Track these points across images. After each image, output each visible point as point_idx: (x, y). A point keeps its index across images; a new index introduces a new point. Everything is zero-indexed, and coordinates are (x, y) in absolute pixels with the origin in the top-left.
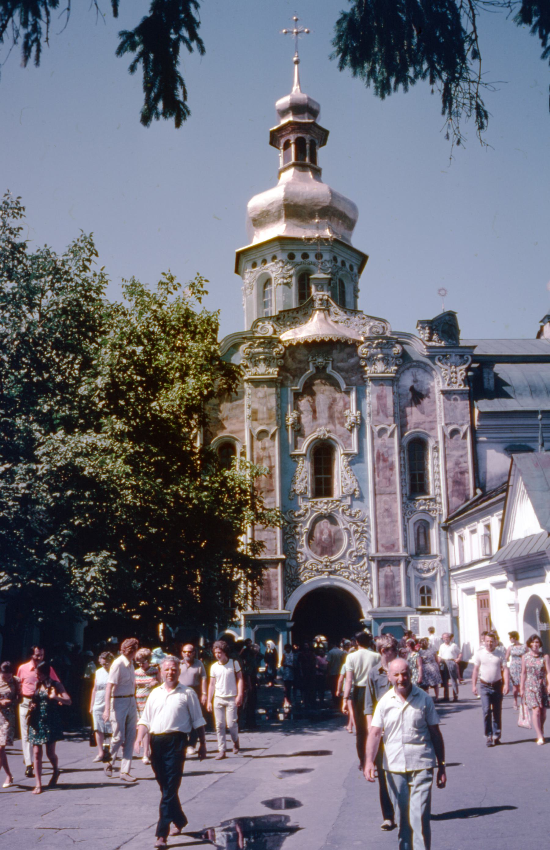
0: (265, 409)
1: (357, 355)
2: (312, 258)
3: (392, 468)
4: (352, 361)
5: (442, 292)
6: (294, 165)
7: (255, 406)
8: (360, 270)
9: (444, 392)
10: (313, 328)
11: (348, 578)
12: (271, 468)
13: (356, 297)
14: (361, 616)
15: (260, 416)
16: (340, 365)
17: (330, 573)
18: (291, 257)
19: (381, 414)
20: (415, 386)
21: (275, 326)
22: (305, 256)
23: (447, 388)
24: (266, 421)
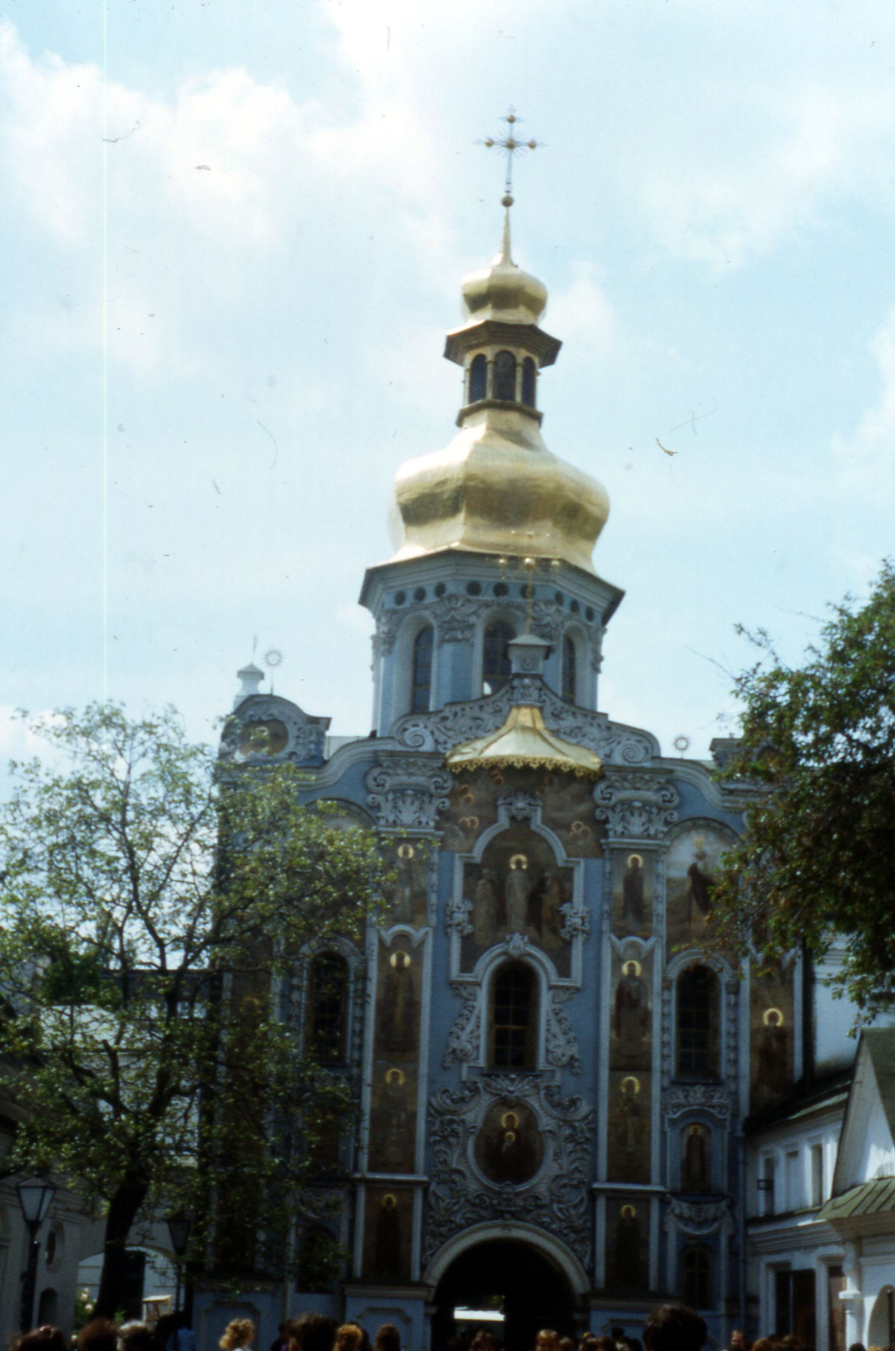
0: (407, 892)
1: (592, 800)
3: (645, 1020)
4: (583, 808)
11: (544, 1227)
13: (596, 670)
16: (556, 815)
18: (474, 588)
19: (630, 916)
20: (700, 866)
21: (436, 733)
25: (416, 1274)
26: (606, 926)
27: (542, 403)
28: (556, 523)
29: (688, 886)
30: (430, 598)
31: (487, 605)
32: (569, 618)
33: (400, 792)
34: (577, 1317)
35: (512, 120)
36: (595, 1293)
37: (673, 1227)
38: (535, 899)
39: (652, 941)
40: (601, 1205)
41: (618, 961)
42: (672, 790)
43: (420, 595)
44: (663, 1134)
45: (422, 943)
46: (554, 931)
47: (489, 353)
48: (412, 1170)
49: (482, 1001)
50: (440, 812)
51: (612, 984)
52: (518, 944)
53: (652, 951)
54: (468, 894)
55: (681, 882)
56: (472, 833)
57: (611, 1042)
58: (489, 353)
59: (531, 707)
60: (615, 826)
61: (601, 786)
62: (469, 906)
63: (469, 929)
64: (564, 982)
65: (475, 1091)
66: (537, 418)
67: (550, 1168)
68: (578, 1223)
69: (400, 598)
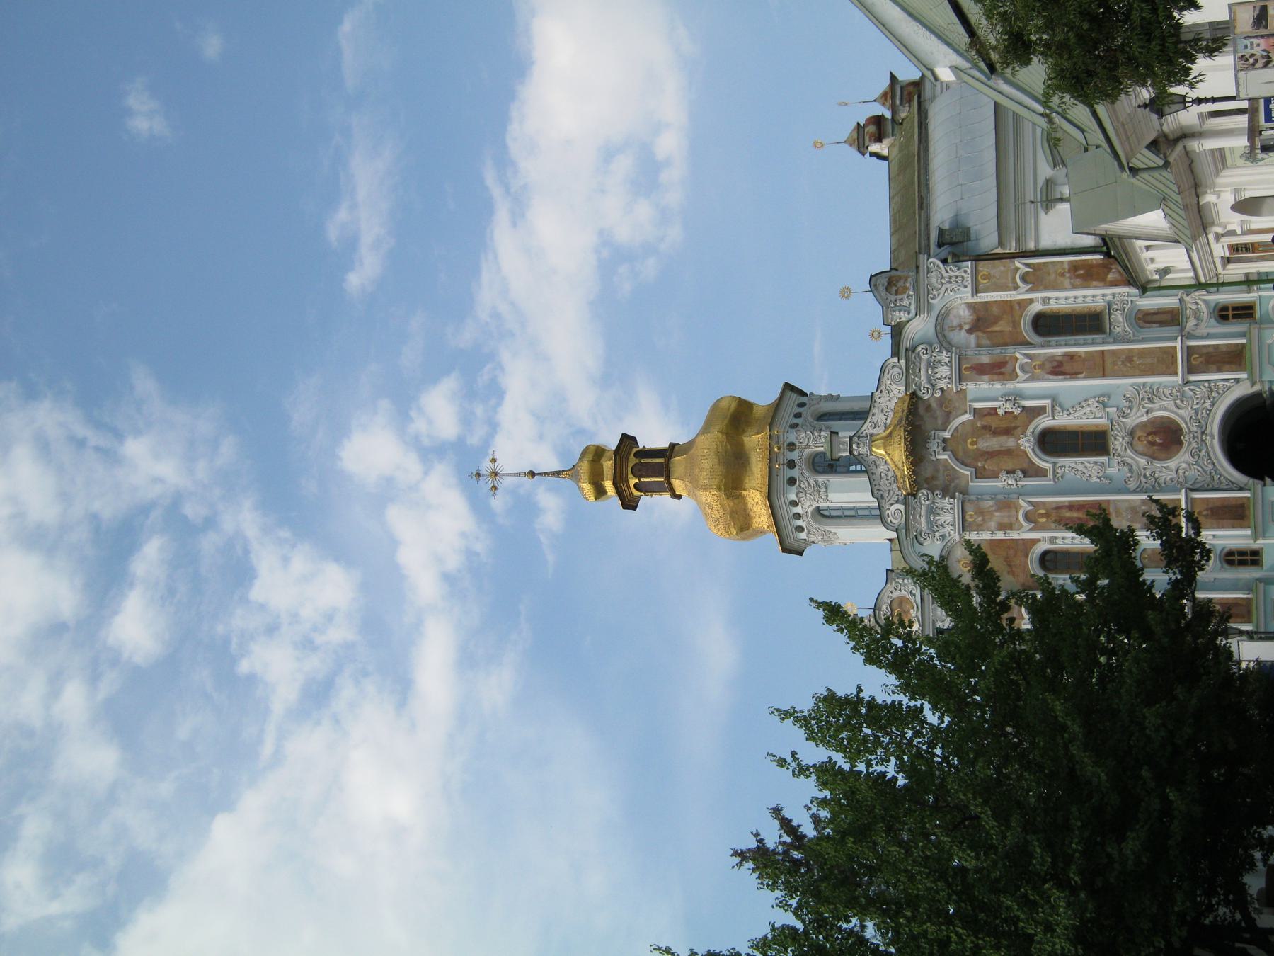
2: (794, 455)
3: (1071, 357)
4: (934, 405)
5: (846, 293)
6: (668, 479)
7: (993, 524)
8: (803, 394)
9: (976, 291)
10: (892, 458)
12: (1071, 507)
14: (1257, 395)
15: (1006, 520)
16: (940, 422)
17: (1203, 433)
18: (792, 481)
20: (967, 327)
22: (791, 464)
23: (969, 288)
24: (1013, 512)
26: (1010, 386)
28: (744, 431)
29: (980, 334)
30: (798, 510)
31: (802, 474)
32: (806, 420)
35: (479, 475)
37: (1203, 331)
38: (996, 432)
39: (1017, 355)
40: (1192, 378)
41: (1033, 379)
42: (919, 349)
43: (798, 516)
44: (1144, 340)
45: (1030, 503)
46: (1016, 417)
47: (633, 481)
48: (1179, 500)
49: (1063, 461)
50: (943, 497)
51: (1048, 380)
53: (1027, 356)
55: (978, 337)
56: (954, 475)
57: (1086, 378)
58: (633, 481)
60: (943, 384)
61: (919, 394)
62: (1003, 476)
64: (1049, 409)
66: (673, 445)
69: (800, 529)
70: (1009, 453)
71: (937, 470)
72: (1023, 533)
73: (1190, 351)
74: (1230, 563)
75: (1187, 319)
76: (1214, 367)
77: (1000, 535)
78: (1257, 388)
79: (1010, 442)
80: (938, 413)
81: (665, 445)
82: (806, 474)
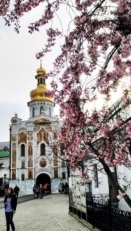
6: (40, 84)
7: (29, 136)
13: (53, 111)
15: (30, 139)
16: (46, 127)
18: (38, 104)
22: (41, 104)
25: (33, 178)
27: (46, 83)
30: (34, 105)
33: (29, 126)
34: (51, 181)
36: (53, 178)
38: (44, 137)
43: (33, 105)
47: (40, 78)
49: (39, 148)
52: (43, 142)
54: (37, 137)
58: (40, 78)
59: (43, 116)
61: (51, 124)
63: (38, 140)
65: (39, 157)
67: (47, 165)
68: (51, 171)
69: (31, 106)
70: (41, 139)
71: (38, 127)
72: (28, 142)
73: (57, 168)
74: (22, 175)
75: (63, 168)
76: (55, 172)
77: (27, 138)
78: (51, 179)
79: (43, 139)
80: (48, 127)
81: (46, 84)
82: (40, 106)
